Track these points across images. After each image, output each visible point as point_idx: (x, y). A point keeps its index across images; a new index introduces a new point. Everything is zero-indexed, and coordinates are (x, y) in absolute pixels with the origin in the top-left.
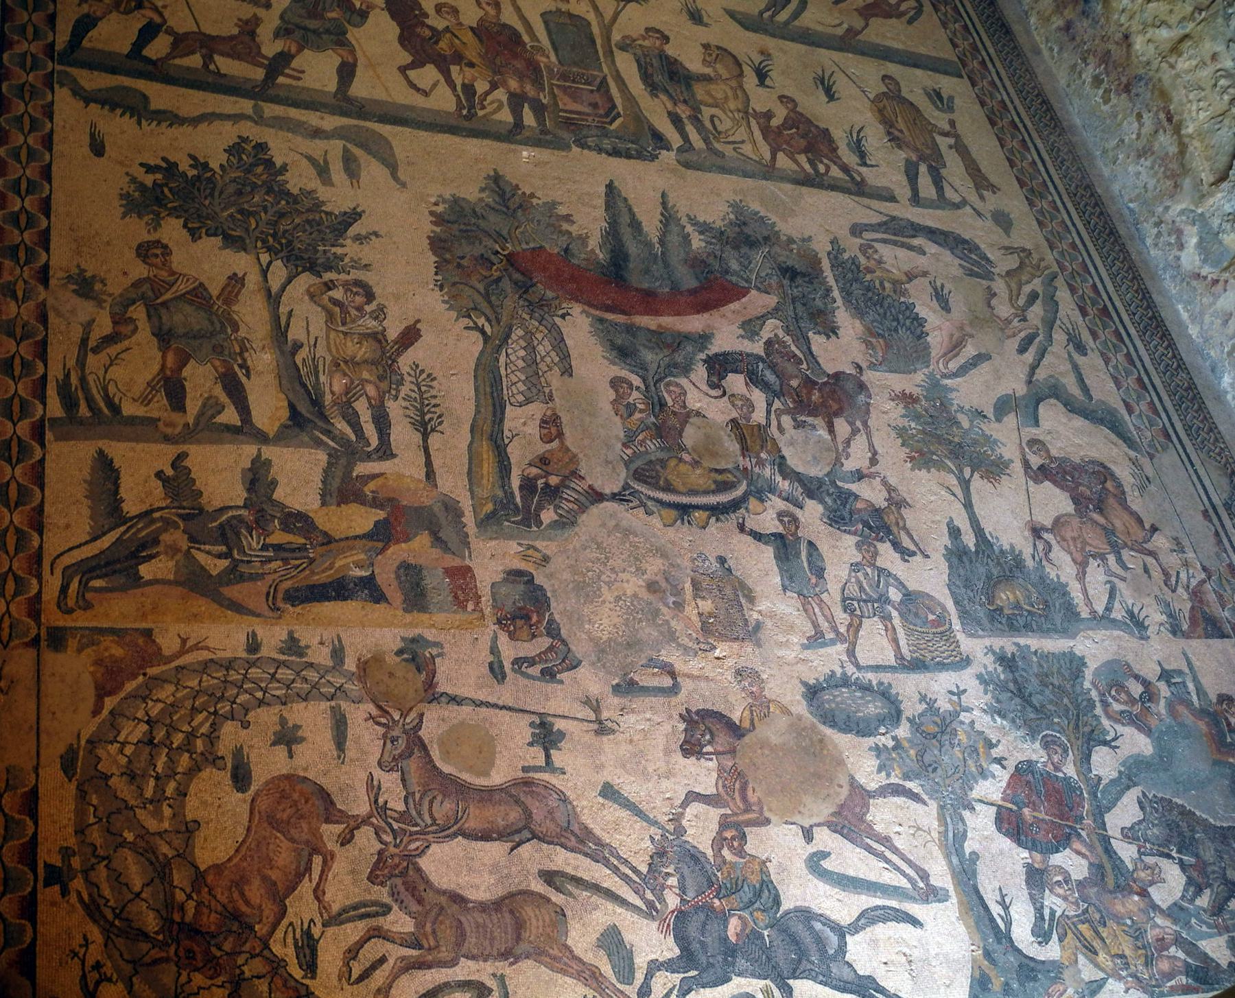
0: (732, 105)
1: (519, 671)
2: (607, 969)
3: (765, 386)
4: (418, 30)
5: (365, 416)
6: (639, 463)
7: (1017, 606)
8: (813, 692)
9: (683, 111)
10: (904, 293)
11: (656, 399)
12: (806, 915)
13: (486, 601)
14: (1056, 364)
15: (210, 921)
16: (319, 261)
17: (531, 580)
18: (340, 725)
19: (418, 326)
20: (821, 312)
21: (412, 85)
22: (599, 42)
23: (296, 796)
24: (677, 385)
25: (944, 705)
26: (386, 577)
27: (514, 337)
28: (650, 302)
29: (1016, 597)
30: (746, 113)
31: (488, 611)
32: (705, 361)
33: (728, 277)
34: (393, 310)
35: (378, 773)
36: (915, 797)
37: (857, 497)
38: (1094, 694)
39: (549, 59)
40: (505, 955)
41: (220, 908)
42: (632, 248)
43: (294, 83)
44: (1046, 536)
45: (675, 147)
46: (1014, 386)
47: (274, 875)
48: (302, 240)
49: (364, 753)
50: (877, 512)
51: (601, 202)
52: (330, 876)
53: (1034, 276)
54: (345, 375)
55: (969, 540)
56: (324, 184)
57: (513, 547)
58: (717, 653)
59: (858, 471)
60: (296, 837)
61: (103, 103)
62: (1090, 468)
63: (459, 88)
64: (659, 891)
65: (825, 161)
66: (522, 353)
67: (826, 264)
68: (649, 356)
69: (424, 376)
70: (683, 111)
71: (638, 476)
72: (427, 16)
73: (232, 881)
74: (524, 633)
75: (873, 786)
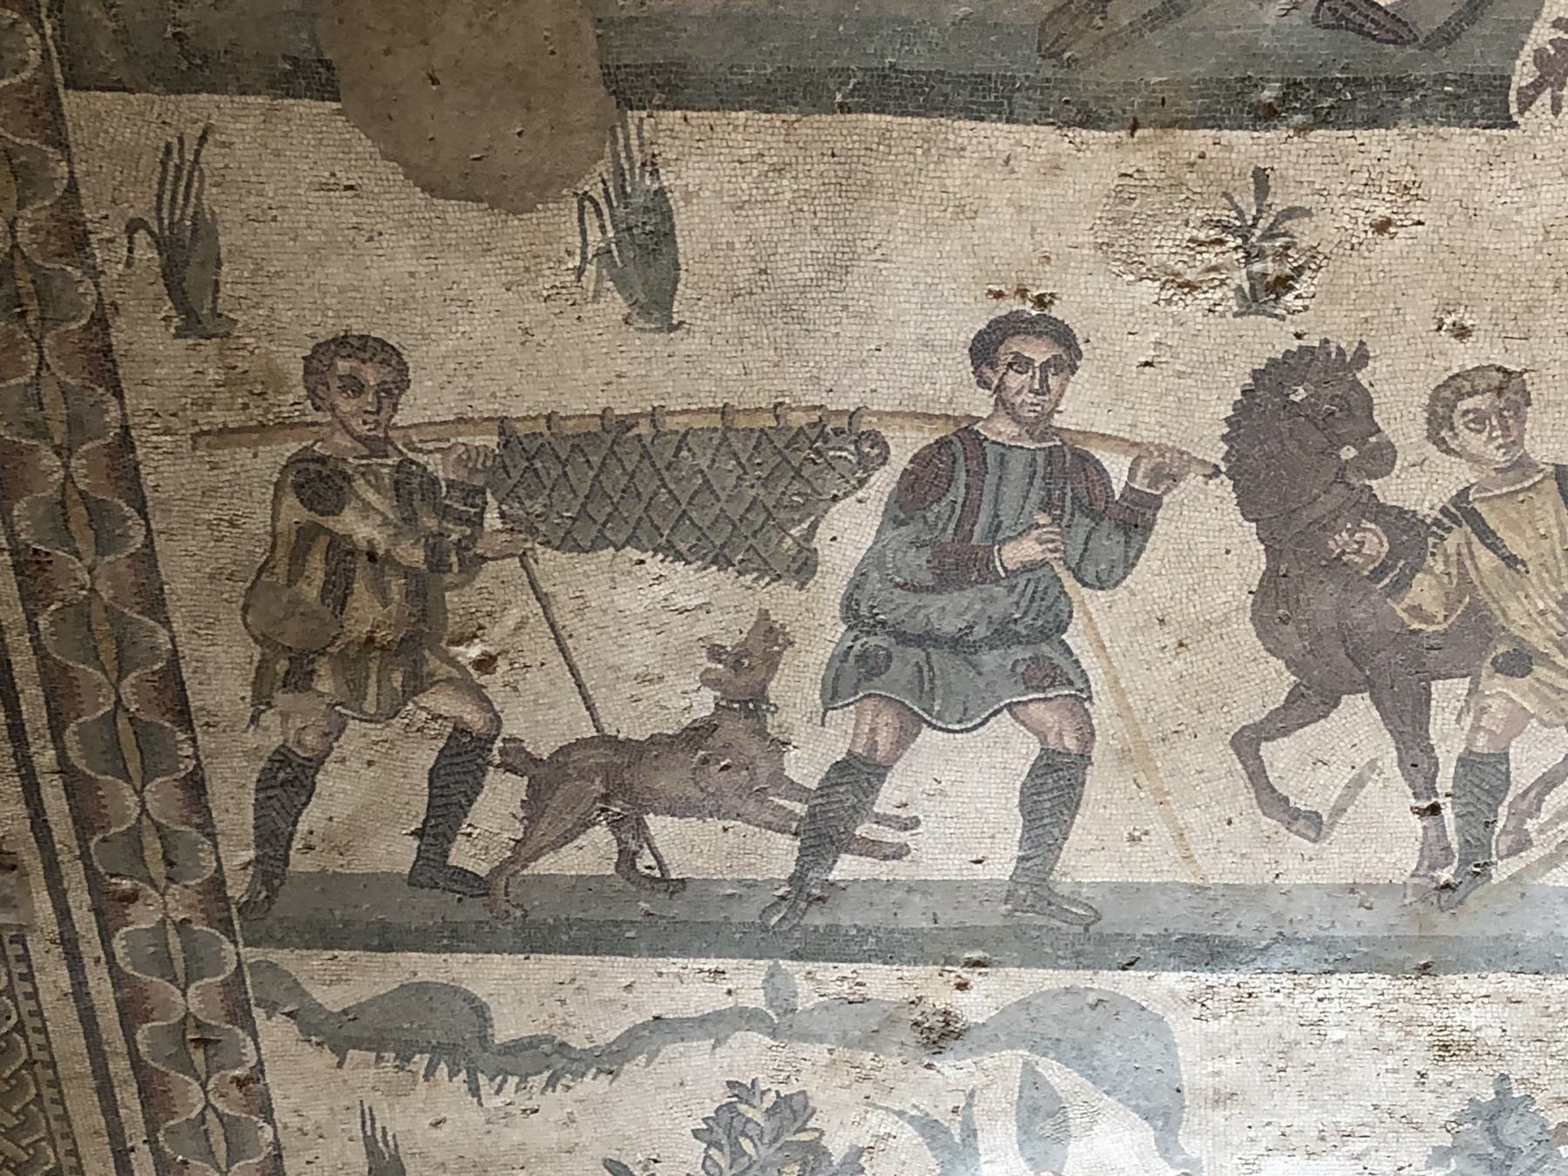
4: (1339, 541)
61: (376, 1044)
72: (1382, 458)
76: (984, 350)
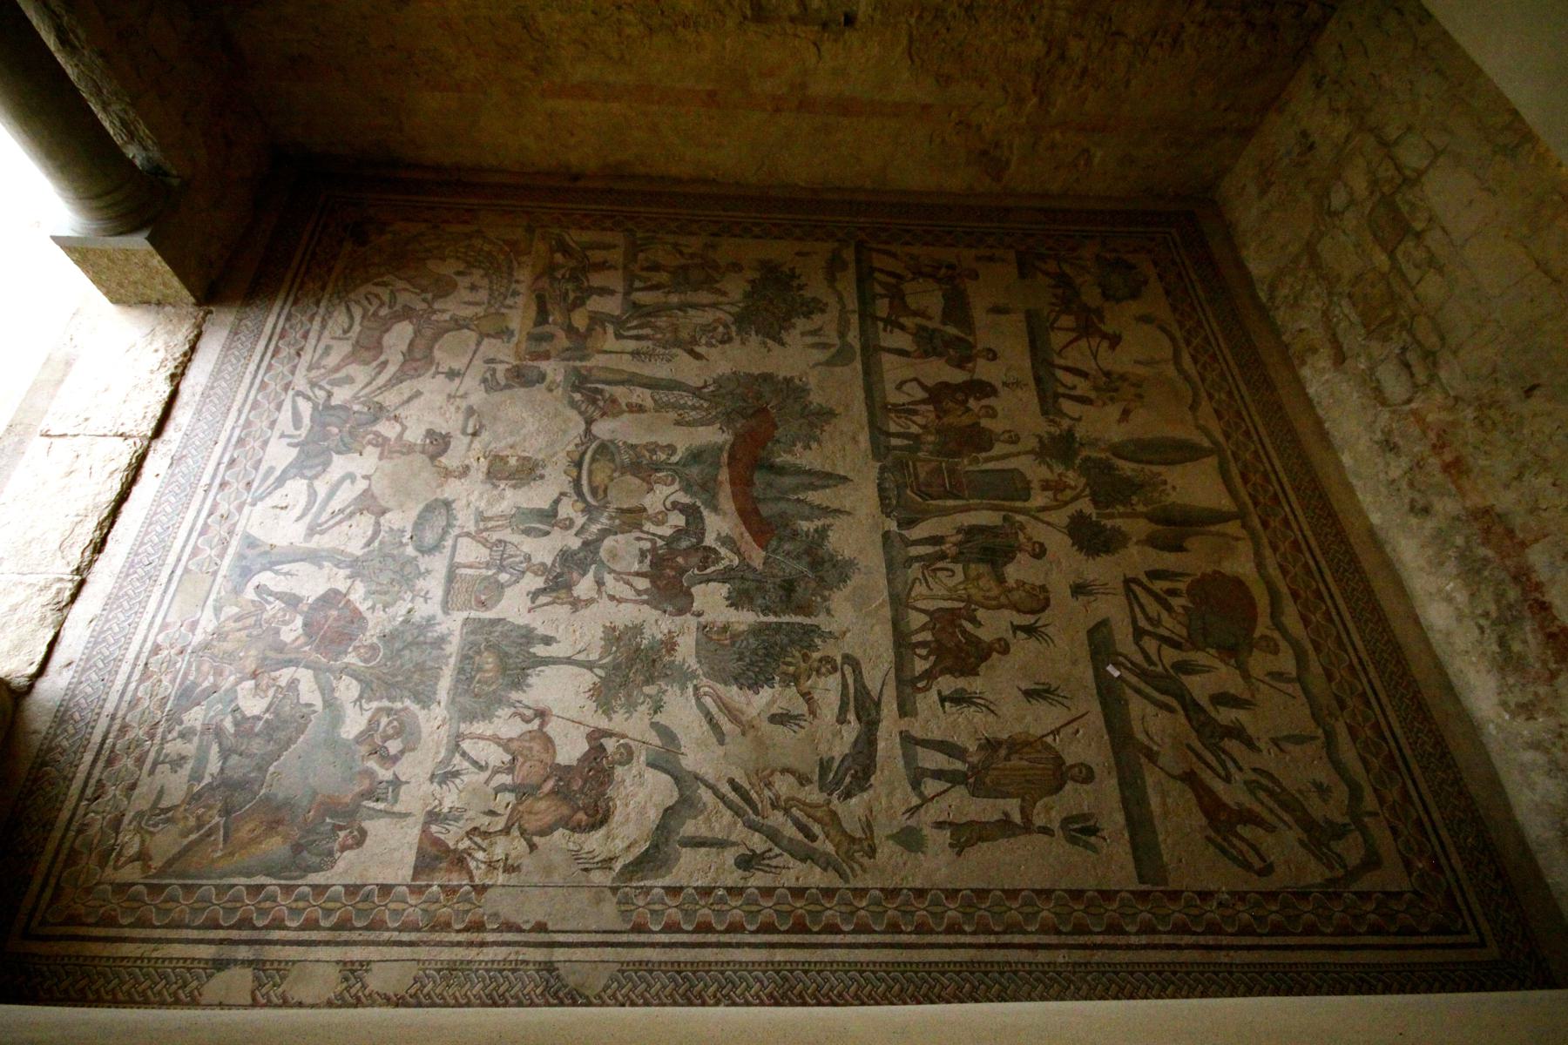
1: (489, 369)
2: (337, 376)
6: (612, 448)
7: (480, 669)
8: (447, 504)
12: (326, 464)
13: (530, 363)
14: (721, 822)
21: (903, 383)
22: (1007, 503)
24: (673, 482)
25: (420, 584)
26: (546, 328)
29: (486, 671)
32: (694, 504)
36: (368, 544)
37: (583, 575)
38: (398, 705)
39: (965, 464)
40: (357, 342)
42: (788, 481)
44: (536, 723)
46: (691, 756)
50: (569, 587)
51: (828, 468)
53: (837, 846)
55: (540, 650)
57: (559, 378)
58: (482, 460)
59: (604, 584)
62: (601, 803)
64: (364, 403)
65: (932, 658)
66: (690, 403)
72: (978, 399)
75: (382, 520)
76: (990, 350)
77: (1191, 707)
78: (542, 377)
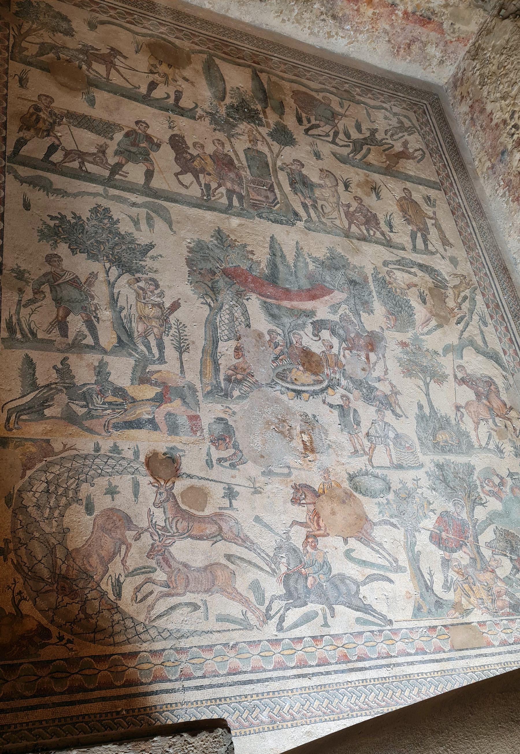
0: (331, 200)
3: (339, 336)
5: (153, 343)
9: (309, 202)
10: (406, 294)
11: (288, 341)
15: (73, 574)
16: (134, 268)
17: (227, 423)
18: (136, 485)
19: (179, 301)
20: (367, 302)
22: (270, 165)
23: (115, 518)
24: (299, 334)
26: (160, 418)
27: (224, 308)
28: (287, 294)
30: (338, 204)
31: (207, 436)
32: (312, 323)
33: (325, 284)
34: (167, 293)
35: (153, 509)
39: (246, 174)
41: (78, 568)
43: (123, 178)
45: (304, 219)
47: (103, 553)
48: (126, 257)
49: (146, 499)
51: (267, 245)
52: (129, 555)
54: (144, 323)
56: (137, 230)
57: (219, 407)
60: (114, 536)
63: (203, 185)
65: (374, 229)
66: (227, 316)
67: (370, 279)
68: (286, 320)
69: (181, 325)
70: (309, 202)
71: (278, 376)
72: (188, 148)
73: (84, 556)
74: (223, 446)
76: (137, 123)
77: (365, 141)
78: (220, 420)
